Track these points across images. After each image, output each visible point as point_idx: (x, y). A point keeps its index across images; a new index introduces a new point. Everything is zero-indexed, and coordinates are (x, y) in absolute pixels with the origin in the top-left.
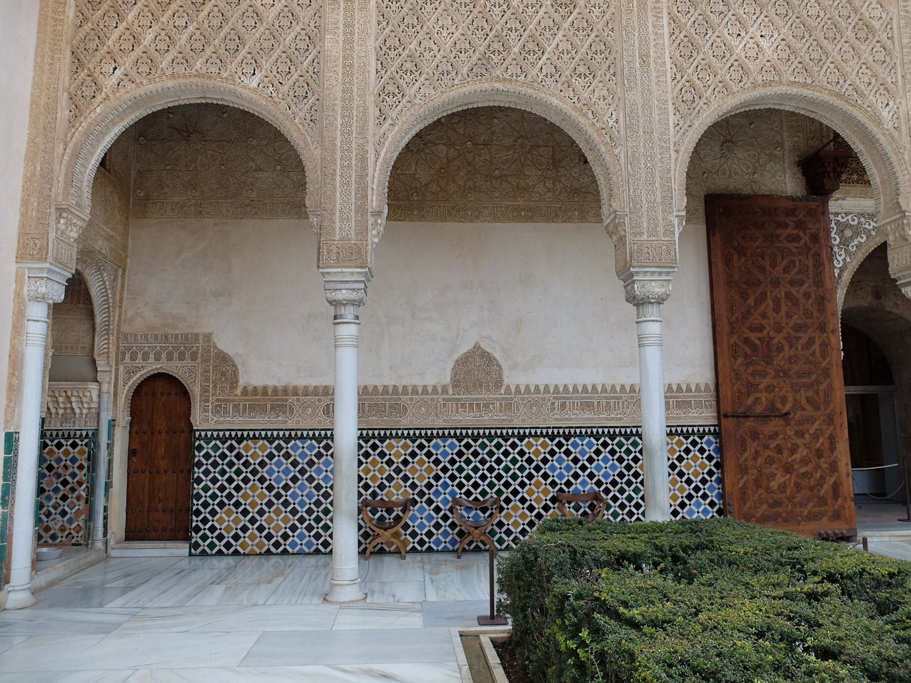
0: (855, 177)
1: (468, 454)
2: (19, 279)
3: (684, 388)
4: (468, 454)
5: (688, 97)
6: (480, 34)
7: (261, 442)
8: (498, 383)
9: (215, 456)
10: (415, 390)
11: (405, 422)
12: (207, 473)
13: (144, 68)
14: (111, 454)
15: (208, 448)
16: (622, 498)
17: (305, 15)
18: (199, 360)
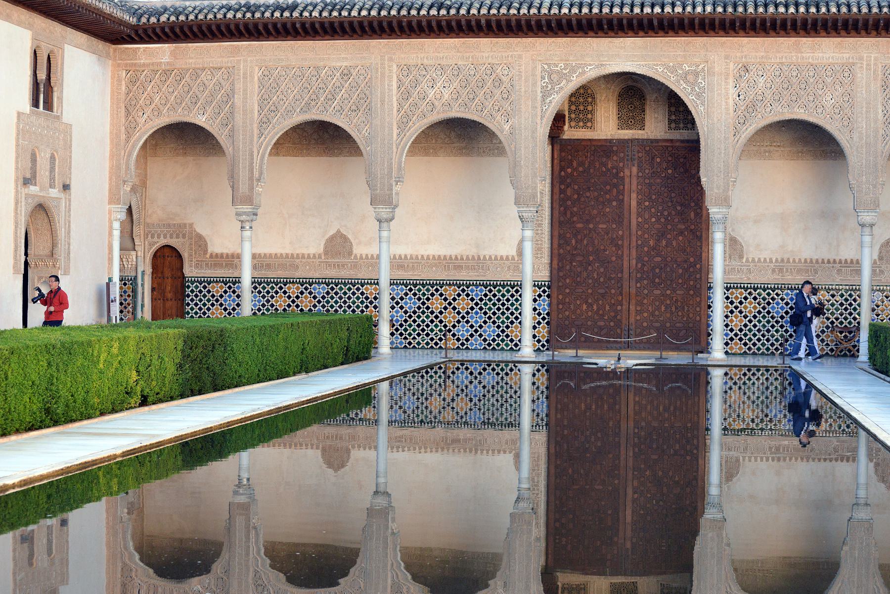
0: (581, 124)
1: (332, 293)
2: (110, 212)
3: (459, 258)
4: (332, 293)
5: (405, 120)
6: (306, 91)
7: (220, 284)
8: (350, 253)
9: (196, 291)
10: (303, 256)
11: (299, 274)
12: (192, 300)
13: (156, 113)
14: (143, 289)
15: (192, 287)
16: (419, 321)
17: (227, 86)
18: (187, 239)
